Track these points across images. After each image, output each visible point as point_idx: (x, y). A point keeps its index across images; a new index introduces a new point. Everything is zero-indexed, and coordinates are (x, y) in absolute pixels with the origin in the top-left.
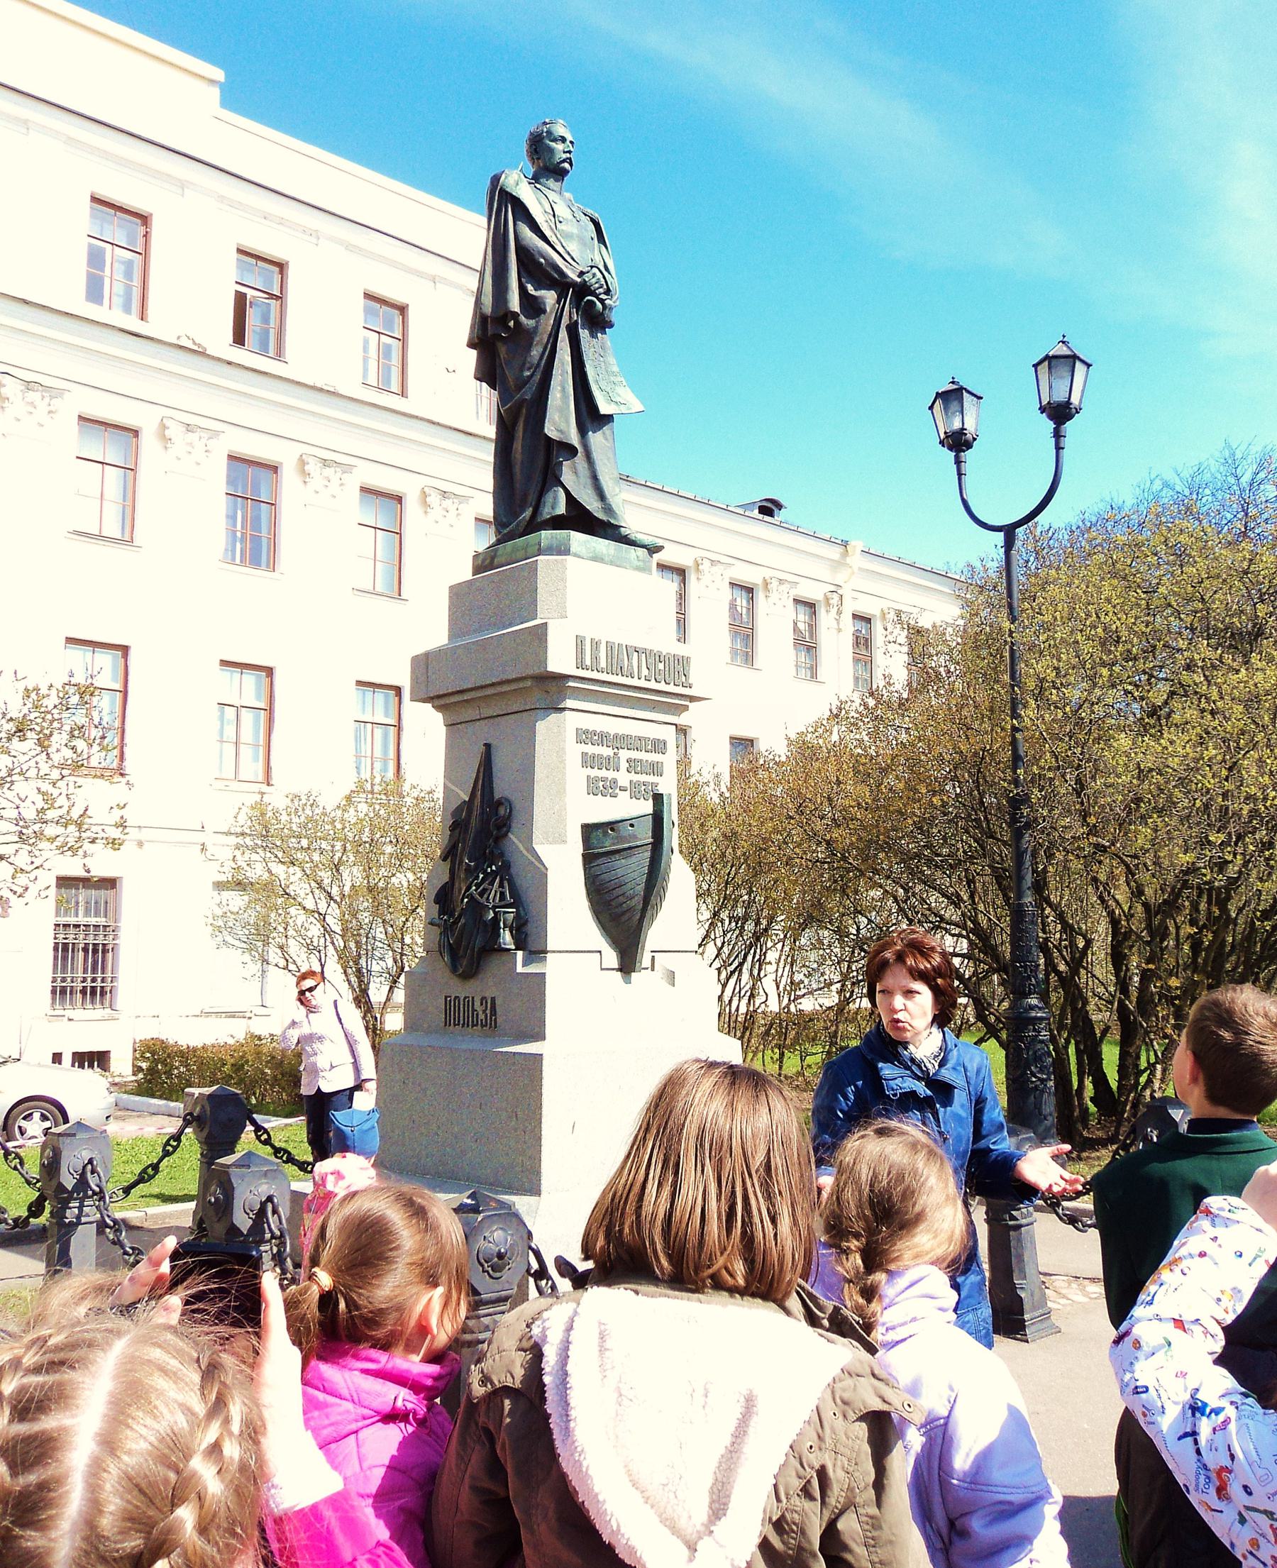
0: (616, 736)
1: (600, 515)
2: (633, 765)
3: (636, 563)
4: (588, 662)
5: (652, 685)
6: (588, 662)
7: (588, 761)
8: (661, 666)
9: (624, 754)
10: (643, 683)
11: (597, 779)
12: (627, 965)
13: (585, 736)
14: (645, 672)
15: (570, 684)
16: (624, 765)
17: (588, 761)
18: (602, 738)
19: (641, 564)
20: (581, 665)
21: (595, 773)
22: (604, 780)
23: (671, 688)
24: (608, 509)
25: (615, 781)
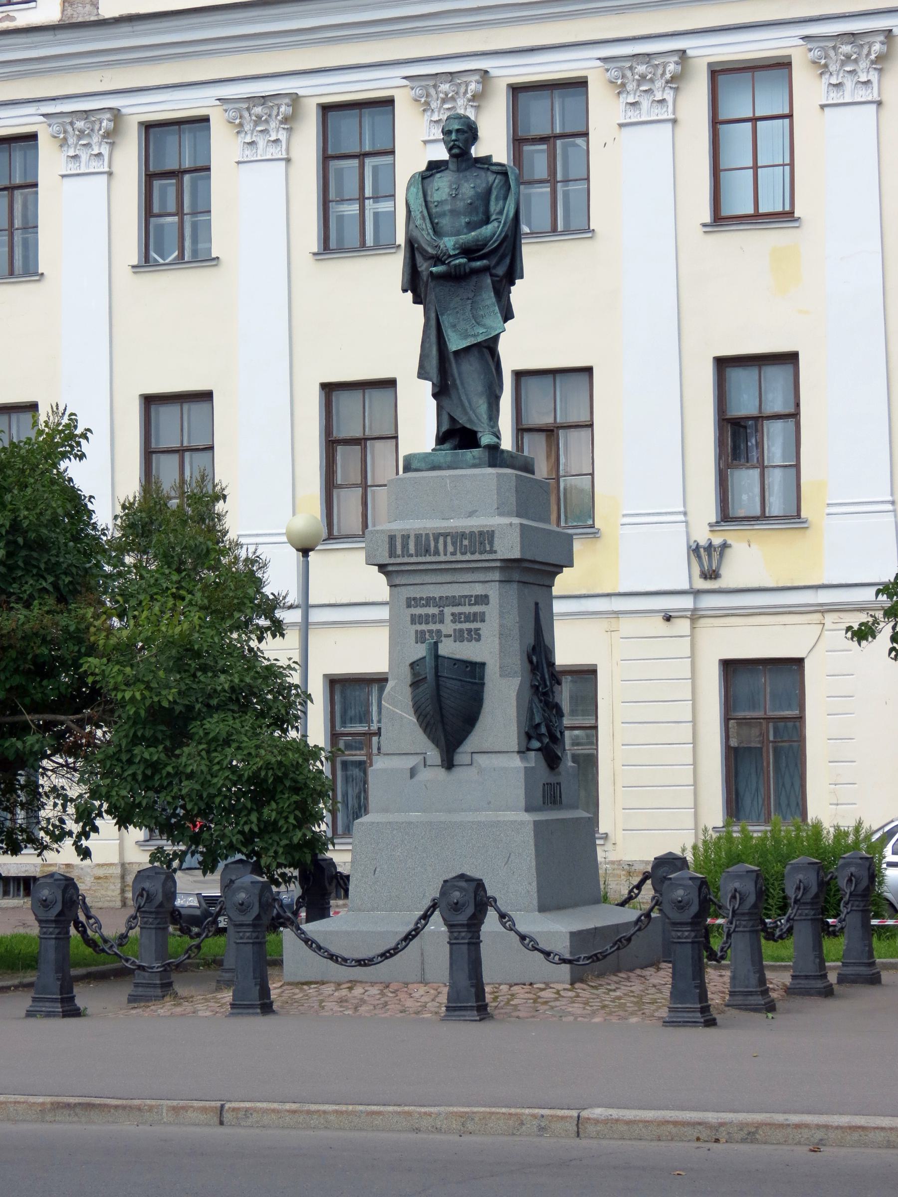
0: (441, 598)
1: (468, 426)
2: (456, 618)
3: (472, 462)
4: (399, 552)
5: (459, 557)
6: (399, 552)
7: (414, 619)
8: (466, 542)
9: (448, 611)
10: (449, 558)
11: (423, 632)
12: (449, 764)
13: (411, 602)
14: (450, 549)
15: (390, 568)
16: (448, 618)
17: (414, 619)
18: (429, 601)
19: (477, 461)
20: (392, 553)
21: (423, 627)
22: (431, 631)
23: (477, 557)
24: (470, 420)
25: (439, 632)
